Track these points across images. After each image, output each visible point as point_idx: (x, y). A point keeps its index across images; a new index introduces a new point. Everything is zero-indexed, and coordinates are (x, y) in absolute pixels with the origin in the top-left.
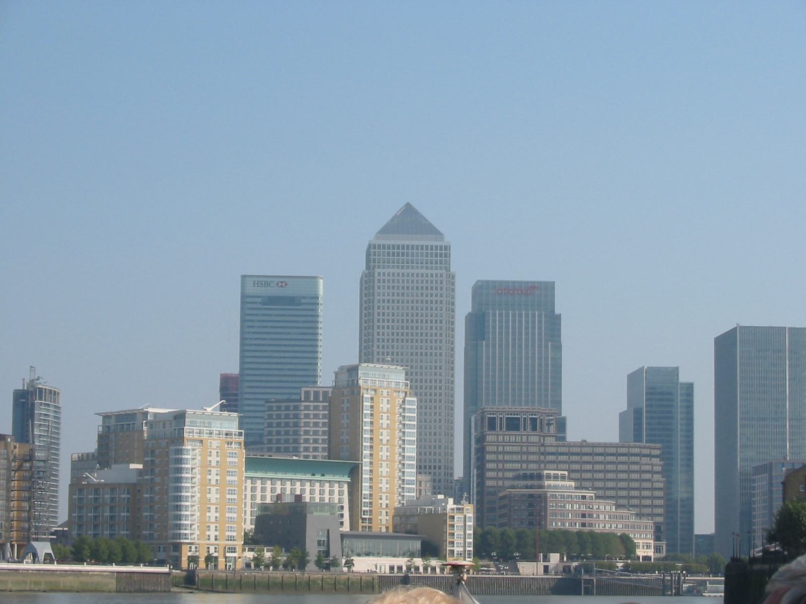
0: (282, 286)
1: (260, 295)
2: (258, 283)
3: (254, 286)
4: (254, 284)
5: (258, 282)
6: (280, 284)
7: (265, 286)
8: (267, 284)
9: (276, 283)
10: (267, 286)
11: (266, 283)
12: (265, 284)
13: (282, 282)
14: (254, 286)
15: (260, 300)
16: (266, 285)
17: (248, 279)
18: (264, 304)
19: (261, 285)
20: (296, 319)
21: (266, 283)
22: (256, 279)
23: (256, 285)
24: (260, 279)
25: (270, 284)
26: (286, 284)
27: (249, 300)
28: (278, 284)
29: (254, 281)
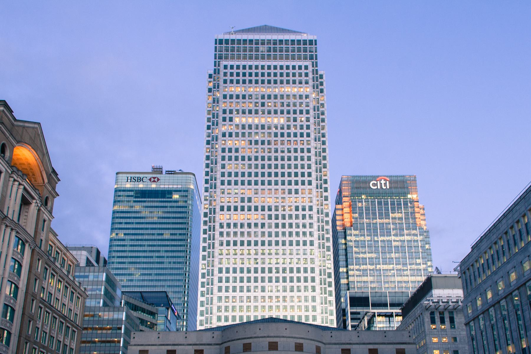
0: (154, 181)
1: (133, 189)
2: (131, 179)
3: (127, 181)
4: (128, 179)
5: (131, 177)
6: (152, 180)
7: (138, 181)
8: (140, 180)
9: (149, 178)
11: (139, 178)
13: (154, 178)
14: (127, 181)
15: (132, 193)
16: (139, 181)
17: (120, 175)
18: (136, 197)
19: (134, 181)
21: (139, 178)
22: (129, 176)
23: (129, 181)
26: (158, 180)
28: (150, 180)
29: (128, 177)
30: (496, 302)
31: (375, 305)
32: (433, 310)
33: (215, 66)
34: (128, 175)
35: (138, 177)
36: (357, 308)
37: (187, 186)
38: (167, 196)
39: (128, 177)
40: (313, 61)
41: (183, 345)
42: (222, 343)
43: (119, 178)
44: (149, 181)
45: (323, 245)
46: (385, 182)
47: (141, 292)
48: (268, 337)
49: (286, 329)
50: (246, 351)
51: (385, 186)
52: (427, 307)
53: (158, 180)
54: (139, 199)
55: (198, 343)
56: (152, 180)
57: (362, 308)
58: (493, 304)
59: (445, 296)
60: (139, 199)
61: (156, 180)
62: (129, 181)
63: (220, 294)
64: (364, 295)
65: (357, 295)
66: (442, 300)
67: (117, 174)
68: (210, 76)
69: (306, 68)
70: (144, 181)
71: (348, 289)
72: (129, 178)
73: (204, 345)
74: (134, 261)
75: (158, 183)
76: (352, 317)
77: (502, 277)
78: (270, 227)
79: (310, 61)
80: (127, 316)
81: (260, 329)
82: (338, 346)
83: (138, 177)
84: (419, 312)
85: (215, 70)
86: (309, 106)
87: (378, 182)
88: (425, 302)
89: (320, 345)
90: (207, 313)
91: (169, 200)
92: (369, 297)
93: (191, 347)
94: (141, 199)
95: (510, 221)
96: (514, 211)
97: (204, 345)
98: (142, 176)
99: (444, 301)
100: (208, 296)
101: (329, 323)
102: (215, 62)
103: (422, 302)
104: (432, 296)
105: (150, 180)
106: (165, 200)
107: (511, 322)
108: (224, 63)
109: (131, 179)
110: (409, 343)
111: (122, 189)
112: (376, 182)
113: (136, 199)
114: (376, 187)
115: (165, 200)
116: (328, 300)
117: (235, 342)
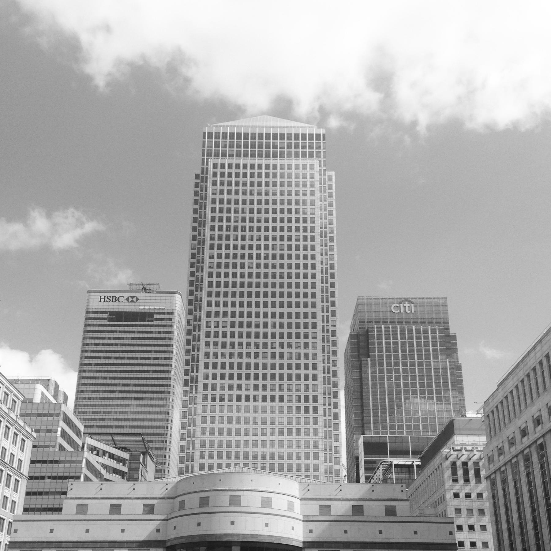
0: (132, 301)
1: (107, 310)
2: (104, 299)
3: (100, 301)
4: (101, 299)
5: (105, 296)
6: (130, 299)
7: (113, 301)
8: (116, 299)
9: (126, 297)
10: (116, 301)
11: (114, 298)
12: (113, 299)
13: (132, 297)
14: (100, 301)
15: (105, 316)
16: (114, 300)
18: (111, 320)
19: (108, 300)
20: (141, 335)
21: (114, 298)
22: (103, 294)
23: (102, 300)
24: (107, 294)
25: (118, 299)
26: (137, 299)
27: (93, 316)
28: (127, 299)
29: (101, 296)
30: (520, 451)
31: (396, 453)
32: (455, 460)
33: (203, 164)
34: (101, 294)
35: (113, 297)
36: (373, 456)
37: (171, 308)
38: (147, 319)
39: (101, 296)
40: (320, 159)
41: (130, 499)
42: (177, 497)
43: (92, 297)
44: (126, 301)
45: (329, 380)
46: (409, 305)
47: (111, 434)
49: (252, 481)
50: (203, 507)
51: (409, 310)
52: (447, 457)
53: (137, 299)
54: (113, 323)
55: (148, 496)
56: (130, 299)
57: (371, 456)
58: (516, 454)
59: (470, 443)
60: (113, 323)
61: (134, 299)
62: (102, 300)
63: (204, 437)
64: (381, 441)
65: (373, 441)
66: (465, 448)
67: (89, 292)
68: (197, 177)
69: (312, 167)
70: (120, 300)
71: (363, 434)
72: (103, 297)
73: (156, 499)
74: (106, 396)
75: (137, 304)
76: (366, 467)
77: (526, 422)
78: (265, 357)
79: (317, 159)
80: (88, 462)
82: (315, 502)
83: (113, 297)
84: (438, 461)
85: (203, 169)
86: (314, 214)
87: (402, 305)
88: (445, 451)
90: (188, 460)
91: (150, 323)
92: (387, 443)
94: (116, 323)
95: (538, 355)
96: (543, 342)
97: (156, 499)
98: (117, 295)
99: (468, 449)
100: (189, 439)
101: (334, 474)
102: (203, 160)
103: (442, 451)
104: (453, 443)
105: (127, 299)
106: (144, 323)
107: (535, 476)
108: (212, 161)
109: (104, 299)
110: (401, 500)
111: (94, 310)
112: (398, 305)
113: (111, 323)
114: (398, 311)
115: (144, 323)
116: (333, 446)
117: (190, 495)
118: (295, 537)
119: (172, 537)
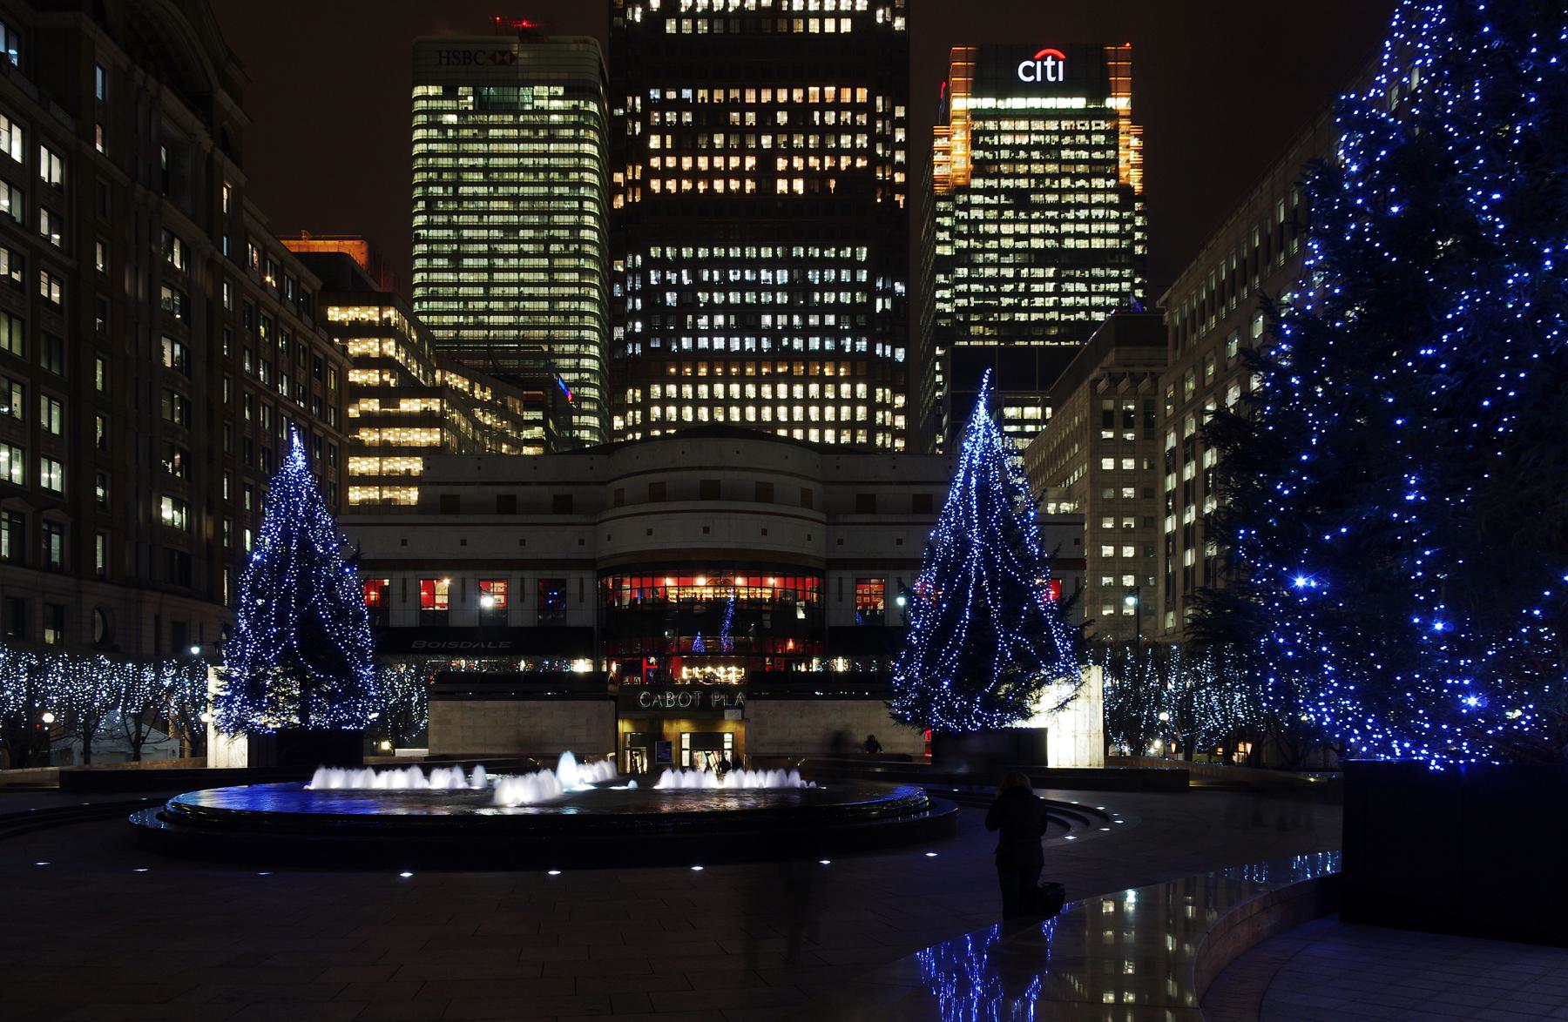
0: (503, 63)
2: (448, 58)
4: (440, 57)
6: (499, 57)
7: (465, 63)
14: (440, 63)
19: (456, 61)
23: (444, 61)
28: (493, 58)
48: (700, 468)
62: (444, 61)
72: (444, 54)
81: (683, 453)
89: (810, 485)
93: (545, 488)
105: (493, 58)
109: (448, 58)
118: (814, 553)
119: (606, 553)
